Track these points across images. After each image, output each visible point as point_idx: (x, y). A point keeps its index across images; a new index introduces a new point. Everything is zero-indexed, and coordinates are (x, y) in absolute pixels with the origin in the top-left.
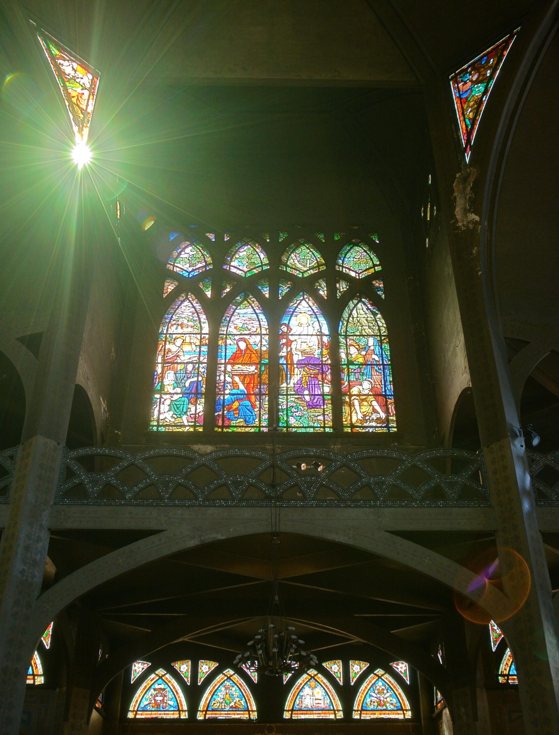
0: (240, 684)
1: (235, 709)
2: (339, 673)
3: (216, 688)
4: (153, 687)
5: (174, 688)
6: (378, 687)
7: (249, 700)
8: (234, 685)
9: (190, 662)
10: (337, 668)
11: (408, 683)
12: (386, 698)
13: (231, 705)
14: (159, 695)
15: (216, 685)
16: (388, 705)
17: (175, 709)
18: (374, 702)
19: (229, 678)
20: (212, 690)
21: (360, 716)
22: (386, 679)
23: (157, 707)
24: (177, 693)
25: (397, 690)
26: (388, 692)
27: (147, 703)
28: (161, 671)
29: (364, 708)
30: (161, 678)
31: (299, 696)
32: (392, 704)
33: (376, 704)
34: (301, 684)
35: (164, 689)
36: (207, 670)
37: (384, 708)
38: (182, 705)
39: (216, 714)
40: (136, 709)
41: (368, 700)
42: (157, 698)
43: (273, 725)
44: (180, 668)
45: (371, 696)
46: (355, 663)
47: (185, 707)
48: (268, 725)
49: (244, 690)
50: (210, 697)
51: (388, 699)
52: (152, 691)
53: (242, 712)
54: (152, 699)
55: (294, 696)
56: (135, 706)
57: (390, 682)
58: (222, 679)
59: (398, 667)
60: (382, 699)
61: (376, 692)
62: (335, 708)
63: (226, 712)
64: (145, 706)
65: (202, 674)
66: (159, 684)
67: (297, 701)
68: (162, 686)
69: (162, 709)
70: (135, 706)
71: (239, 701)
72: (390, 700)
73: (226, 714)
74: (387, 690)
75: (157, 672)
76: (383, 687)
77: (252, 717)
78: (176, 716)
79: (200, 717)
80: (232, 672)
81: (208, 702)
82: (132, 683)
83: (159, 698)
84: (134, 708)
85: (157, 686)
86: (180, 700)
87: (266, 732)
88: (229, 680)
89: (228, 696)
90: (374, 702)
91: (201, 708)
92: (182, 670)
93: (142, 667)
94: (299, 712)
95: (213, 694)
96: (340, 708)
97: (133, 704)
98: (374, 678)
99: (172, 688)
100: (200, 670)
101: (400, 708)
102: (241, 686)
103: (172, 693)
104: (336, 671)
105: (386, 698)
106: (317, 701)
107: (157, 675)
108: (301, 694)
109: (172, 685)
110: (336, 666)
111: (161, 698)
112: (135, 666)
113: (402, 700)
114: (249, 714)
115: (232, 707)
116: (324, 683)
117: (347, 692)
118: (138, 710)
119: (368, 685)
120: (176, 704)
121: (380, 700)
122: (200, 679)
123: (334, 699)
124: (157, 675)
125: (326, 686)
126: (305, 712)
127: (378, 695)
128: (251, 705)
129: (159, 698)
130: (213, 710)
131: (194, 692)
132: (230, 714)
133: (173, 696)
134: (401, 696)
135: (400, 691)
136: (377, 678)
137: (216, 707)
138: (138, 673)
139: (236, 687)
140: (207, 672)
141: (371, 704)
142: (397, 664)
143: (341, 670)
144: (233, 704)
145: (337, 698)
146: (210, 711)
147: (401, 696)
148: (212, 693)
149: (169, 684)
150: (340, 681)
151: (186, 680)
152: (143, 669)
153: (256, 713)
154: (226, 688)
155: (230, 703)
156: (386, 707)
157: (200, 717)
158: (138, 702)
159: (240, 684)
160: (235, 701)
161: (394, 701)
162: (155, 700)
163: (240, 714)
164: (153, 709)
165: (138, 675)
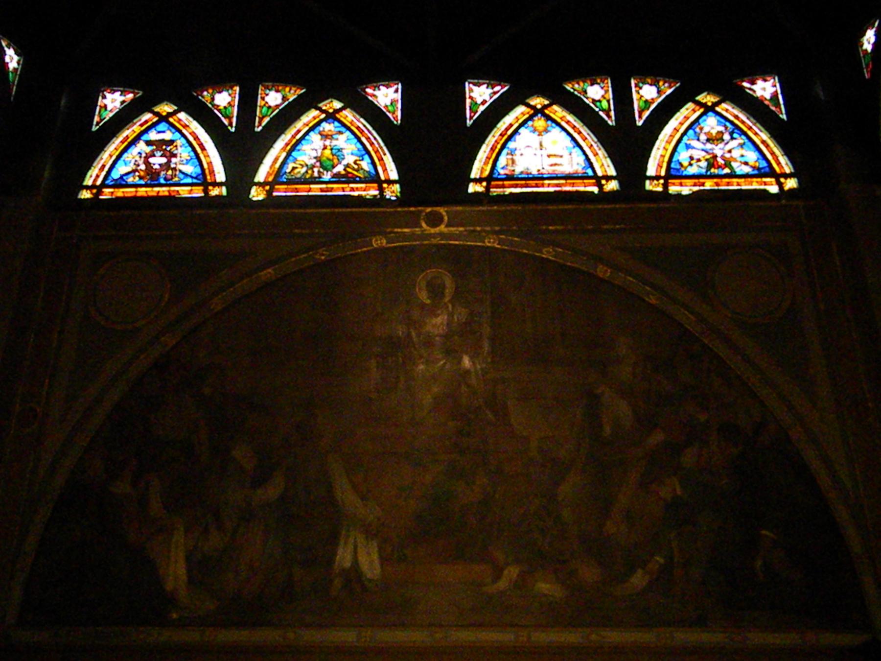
0: (358, 128)
1: (346, 178)
2: (605, 104)
3: (298, 137)
4: (145, 137)
5: (196, 138)
6: (706, 130)
7: (381, 159)
8: (343, 129)
9: (237, 89)
10: (602, 92)
11: (784, 117)
12: (730, 151)
13: (335, 170)
14: (159, 154)
15: (299, 131)
16: (734, 165)
17: (195, 181)
18: (699, 160)
19: (331, 117)
20: (290, 141)
21: (666, 186)
22: (727, 110)
23: (151, 179)
24: (203, 149)
25: (756, 134)
26: (732, 138)
27: (129, 169)
28: (166, 108)
29: (673, 172)
30: (164, 119)
31: (505, 151)
32: (746, 163)
33: (704, 164)
34: (511, 125)
35: (171, 142)
36: (279, 101)
37: (727, 171)
38: (212, 172)
39: (297, 190)
40: (98, 183)
41: (683, 156)
42: (151, 160)
43: (442, 210)
44: (213, 99)
45: (688, 147)
46: (644, 83)
47: (221, 177)
48: (429, 210)
49: (368, 139)
50: (284, 154)
51: (736, 154)
52: (141, 147)
53: (363, 185)
54: (141, 162)
55: (492, 149)
56: (98, 176)
57: (737, 117)
58: (314, 118)
59: (754, 87)
60: (719, 153)
61: (703, 137)
62: (600, 174)
63: (324, 186)
64: (122, 177)
65: (265, 109)
66: (159, 132)
67: (503, 161)
68: (168, 136)
69: (162, 181)
70: (98, 176)
71: (355, 163)
72: (743, 158)
73: (322, 190)
74: (731, 134)
75: (157, 109)
76: (722, 129)
77: (388, 195)
78: (198, 192)
79: (257, 194)
80: (337, 105)
81: (277, 165)
82: (94, 128)
83: (157, 161)
84: (95, 180)
85: (153, 136)
86: (210, 164)
87: (424, 225)
88: (331, 120)
89: (327, 152)
90: (699, 160)
91: (260, 177)
92: (217, 102)
93: (123, 98)
94: (506, 183)
95: (293, 148)
96: (612, 172)
97: (93, 172)
98: (694, 111)
99: (191, 138)
100: (260, 102)
101: (767, 169)
102: (362, 132)
103: (190, 149)
104: (597, 98)
105: (730, 151)
106: (553, 160)
107: (157, 114)
108: (511, 145)
109: (193, 134)
110: (596, 88)
111: (164, 160)
112: (104, 97)
113: (773, 153)
114: (381, 190)
115: (337, 175)
116: (568, 122)
117: (628, 142)
118: (104, 185)
119: (681, 124)
120: (198, 170)
121: (715, 157)
122: (261, 119)
123: (596, 154)
124: (157, 114)
125: (574, 127)
126: (523, 182)
127: (709, 146)
128: (385, 170)
129: (157, 161)
130: (289, 182)
131: (242, 145)
132: (332, 190)
133: (192, 154)
134: (767, 146)
135: (765, 136)
136: (702, 110)
137: (299, 176)
138: (111, 111)
139: (348, 133)
140: (277, 106)
141: (691, 165)
142: (753, 83)
143: (610, 95)
144: (340, 169)
145: (602, 153)
146: (283, 183)
147: (767, 146)
148: (289, 147)
149: (184, 131)
150: (609, 117)
151: (226, 122)
152: (123, 102)
153: (397, 187)
154: (325, 136)
155: (334, 167)
156: (731, 168)
157: (257, 194)
158: (106, 169)
159: (358, 128)
160: (345, 162)
161: (752, 156)
162: (146, 163)
163: (357, 189)
164: (142, 182)
165: (111, 115)
